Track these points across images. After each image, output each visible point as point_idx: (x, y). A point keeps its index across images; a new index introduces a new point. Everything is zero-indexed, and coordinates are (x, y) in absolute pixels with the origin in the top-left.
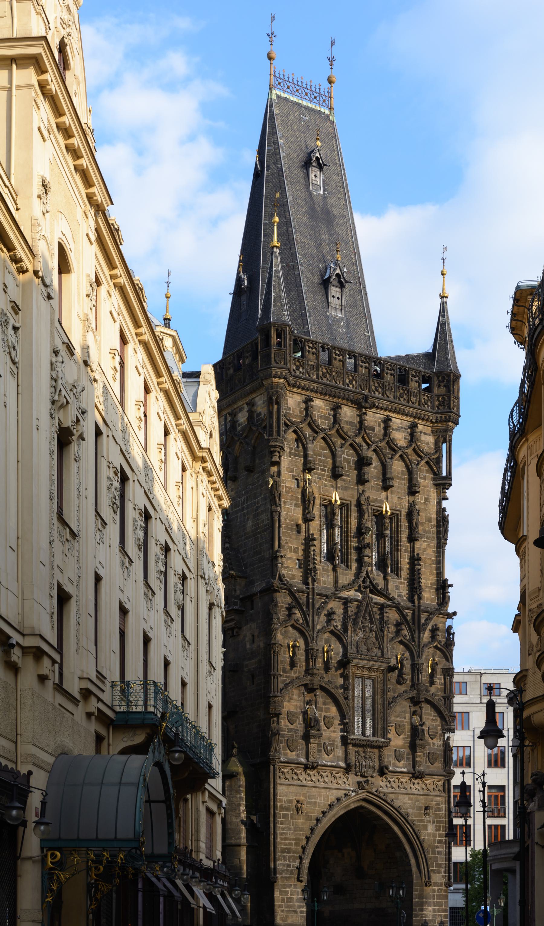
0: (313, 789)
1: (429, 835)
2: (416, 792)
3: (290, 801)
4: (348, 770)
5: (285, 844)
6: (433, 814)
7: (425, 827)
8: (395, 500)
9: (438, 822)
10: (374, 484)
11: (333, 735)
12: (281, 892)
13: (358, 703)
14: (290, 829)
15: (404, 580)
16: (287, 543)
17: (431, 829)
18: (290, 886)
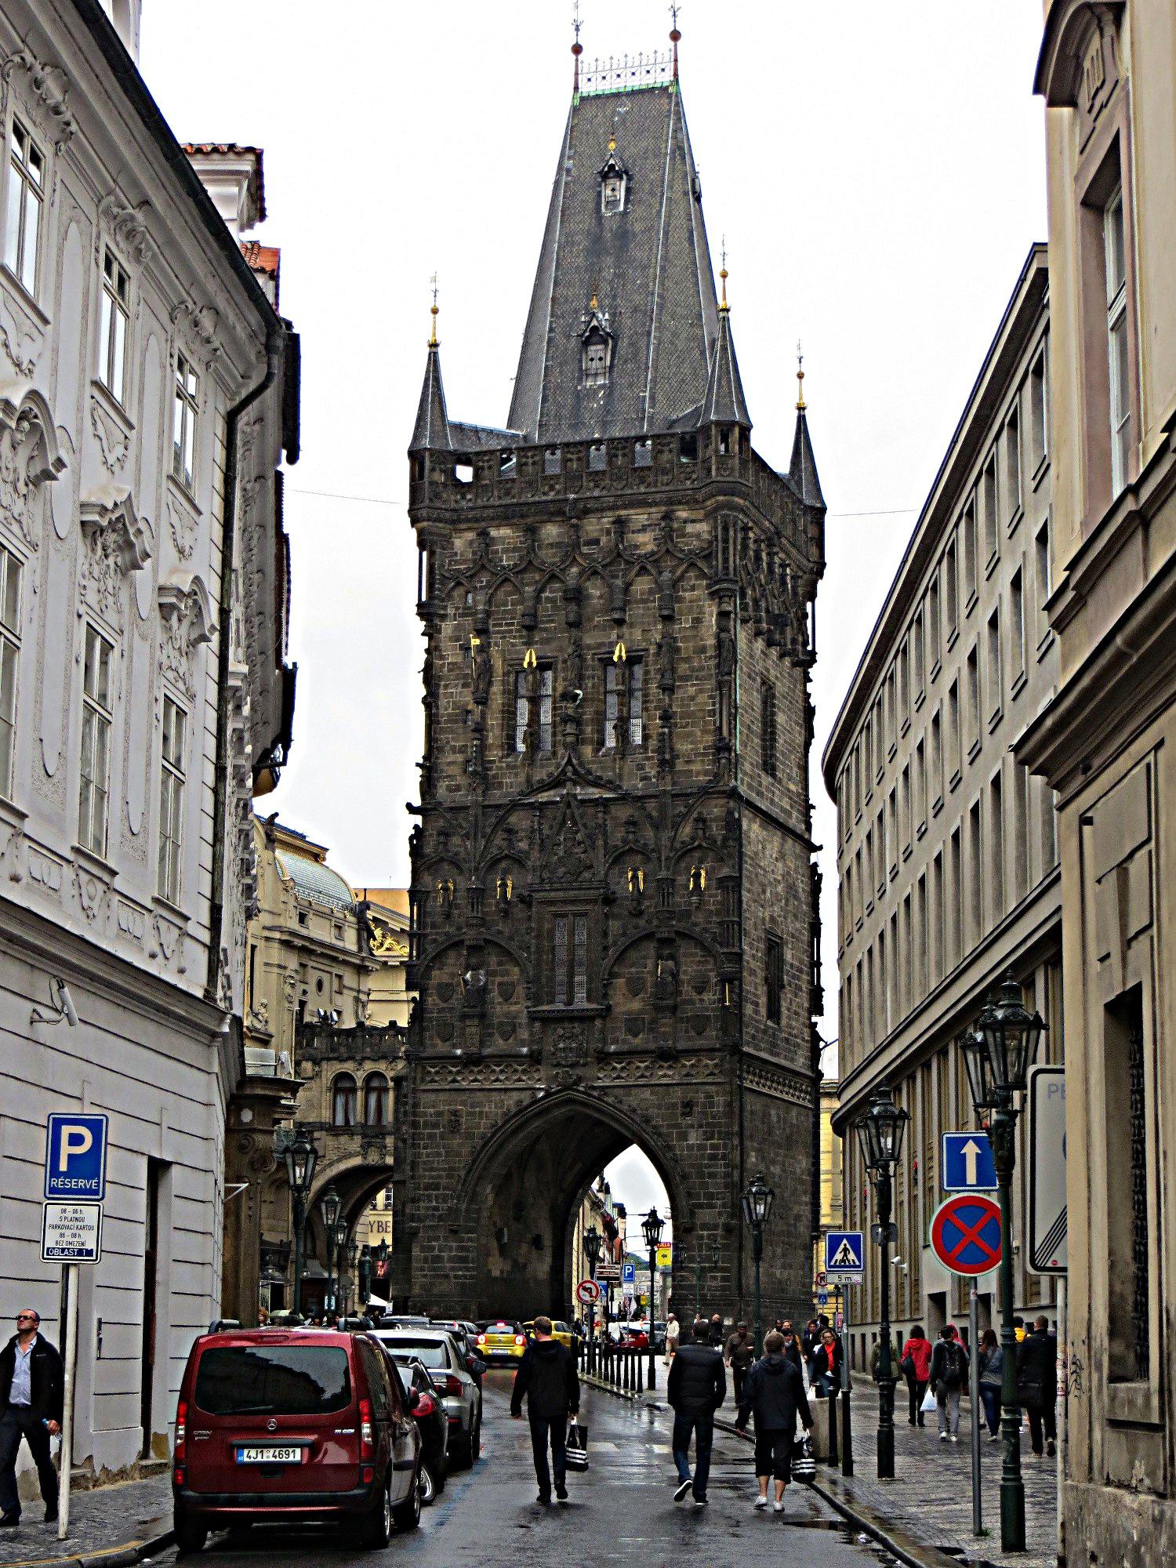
0: (479, 1094)
1: (690, 1147)
2: (664, 1081)
3: (440, 1114)
4: (535, 1059)
5: (432, 1177)
6: (699, 1113)
7: (683, 1136)
8: (638, 634)
9: (708, 1124)
10: (599, 622)
11: (513, 1008)
12: (423, 1249)
13: (562, 954)
14: (439, 1154)
15: (653, 752)
16: (448, 742)
17: (693, 1138)
18: (437, 1239)
